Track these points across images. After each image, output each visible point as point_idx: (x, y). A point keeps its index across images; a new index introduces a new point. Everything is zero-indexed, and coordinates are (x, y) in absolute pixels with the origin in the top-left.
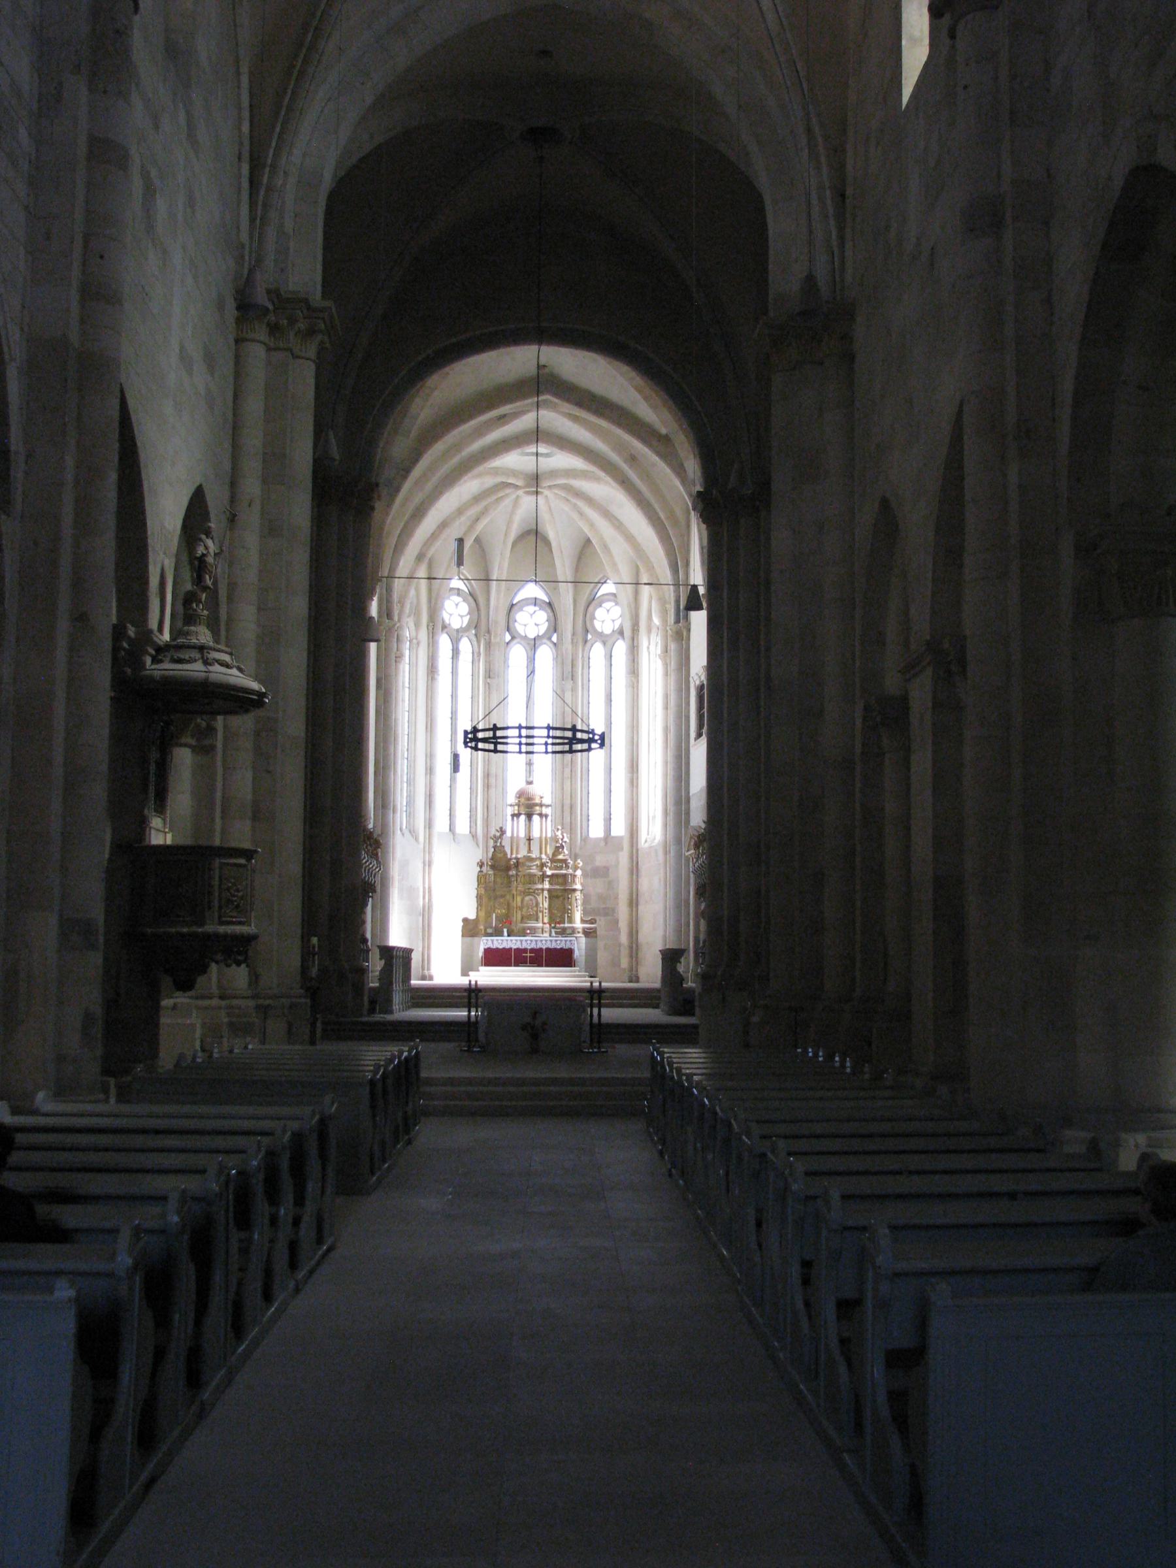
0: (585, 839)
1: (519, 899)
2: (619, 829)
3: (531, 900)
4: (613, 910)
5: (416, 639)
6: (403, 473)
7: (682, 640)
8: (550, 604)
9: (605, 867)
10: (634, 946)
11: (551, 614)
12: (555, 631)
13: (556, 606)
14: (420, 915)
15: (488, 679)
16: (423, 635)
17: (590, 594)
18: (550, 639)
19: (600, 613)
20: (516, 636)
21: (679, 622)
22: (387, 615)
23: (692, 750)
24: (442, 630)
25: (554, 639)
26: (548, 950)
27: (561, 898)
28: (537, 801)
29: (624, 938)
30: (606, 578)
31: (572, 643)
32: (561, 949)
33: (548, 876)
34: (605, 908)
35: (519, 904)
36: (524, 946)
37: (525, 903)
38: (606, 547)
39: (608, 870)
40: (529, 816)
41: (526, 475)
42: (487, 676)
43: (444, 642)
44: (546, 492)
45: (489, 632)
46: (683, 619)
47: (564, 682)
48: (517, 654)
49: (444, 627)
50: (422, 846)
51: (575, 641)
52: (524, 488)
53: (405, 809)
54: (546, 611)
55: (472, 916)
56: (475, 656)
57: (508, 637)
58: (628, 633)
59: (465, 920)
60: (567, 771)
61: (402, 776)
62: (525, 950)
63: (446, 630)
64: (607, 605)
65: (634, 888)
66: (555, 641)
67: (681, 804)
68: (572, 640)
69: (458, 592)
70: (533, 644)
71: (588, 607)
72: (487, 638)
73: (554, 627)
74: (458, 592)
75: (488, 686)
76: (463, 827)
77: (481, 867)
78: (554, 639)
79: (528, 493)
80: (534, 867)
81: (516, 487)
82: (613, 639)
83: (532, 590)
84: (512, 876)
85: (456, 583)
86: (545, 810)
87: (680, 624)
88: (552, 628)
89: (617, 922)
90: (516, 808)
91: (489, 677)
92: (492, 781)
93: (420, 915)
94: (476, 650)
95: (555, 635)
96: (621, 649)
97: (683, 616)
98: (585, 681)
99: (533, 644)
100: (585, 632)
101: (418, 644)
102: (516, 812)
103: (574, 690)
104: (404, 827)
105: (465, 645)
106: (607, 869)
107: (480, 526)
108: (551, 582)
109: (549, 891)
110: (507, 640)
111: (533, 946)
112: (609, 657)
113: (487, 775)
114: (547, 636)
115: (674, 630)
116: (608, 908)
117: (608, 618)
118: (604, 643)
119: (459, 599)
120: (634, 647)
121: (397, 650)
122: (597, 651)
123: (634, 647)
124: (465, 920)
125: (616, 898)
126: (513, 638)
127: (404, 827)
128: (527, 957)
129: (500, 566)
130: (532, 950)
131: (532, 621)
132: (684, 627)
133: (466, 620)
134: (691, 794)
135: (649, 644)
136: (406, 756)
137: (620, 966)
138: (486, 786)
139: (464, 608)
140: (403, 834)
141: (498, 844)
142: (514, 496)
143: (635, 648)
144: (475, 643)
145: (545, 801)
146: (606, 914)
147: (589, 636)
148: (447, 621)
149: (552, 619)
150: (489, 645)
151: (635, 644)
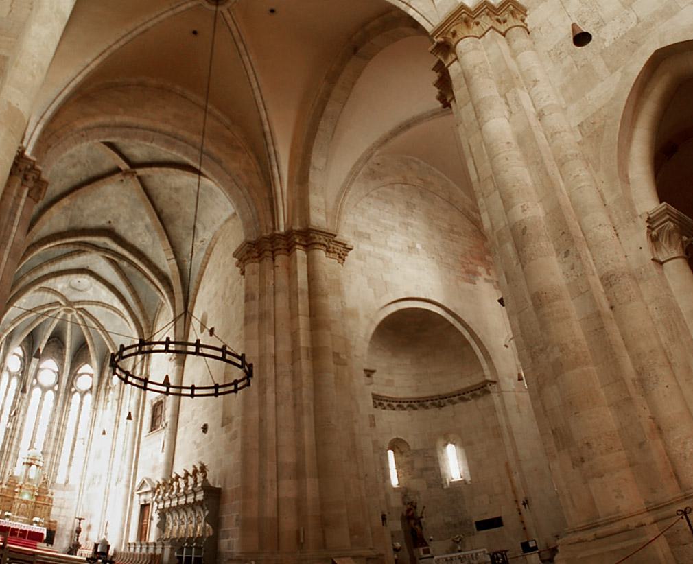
1: (18, 504)
25: (56, 388)
26: (30, 532)
32: (38, 533)
35: (17, 507)
36: (17, 527)
48: (37, 392)
49: (8, 370)
57: (35, 382)
58: (94, 389)
62: (17, 530)
70: (44, 390)
84: (17, 492)
95: (57, 386)
109: (35, 503)
111: (22, 528)
117: (83, 382)
118: (80, 393)
130: (21, 530)
142: (58, 311)
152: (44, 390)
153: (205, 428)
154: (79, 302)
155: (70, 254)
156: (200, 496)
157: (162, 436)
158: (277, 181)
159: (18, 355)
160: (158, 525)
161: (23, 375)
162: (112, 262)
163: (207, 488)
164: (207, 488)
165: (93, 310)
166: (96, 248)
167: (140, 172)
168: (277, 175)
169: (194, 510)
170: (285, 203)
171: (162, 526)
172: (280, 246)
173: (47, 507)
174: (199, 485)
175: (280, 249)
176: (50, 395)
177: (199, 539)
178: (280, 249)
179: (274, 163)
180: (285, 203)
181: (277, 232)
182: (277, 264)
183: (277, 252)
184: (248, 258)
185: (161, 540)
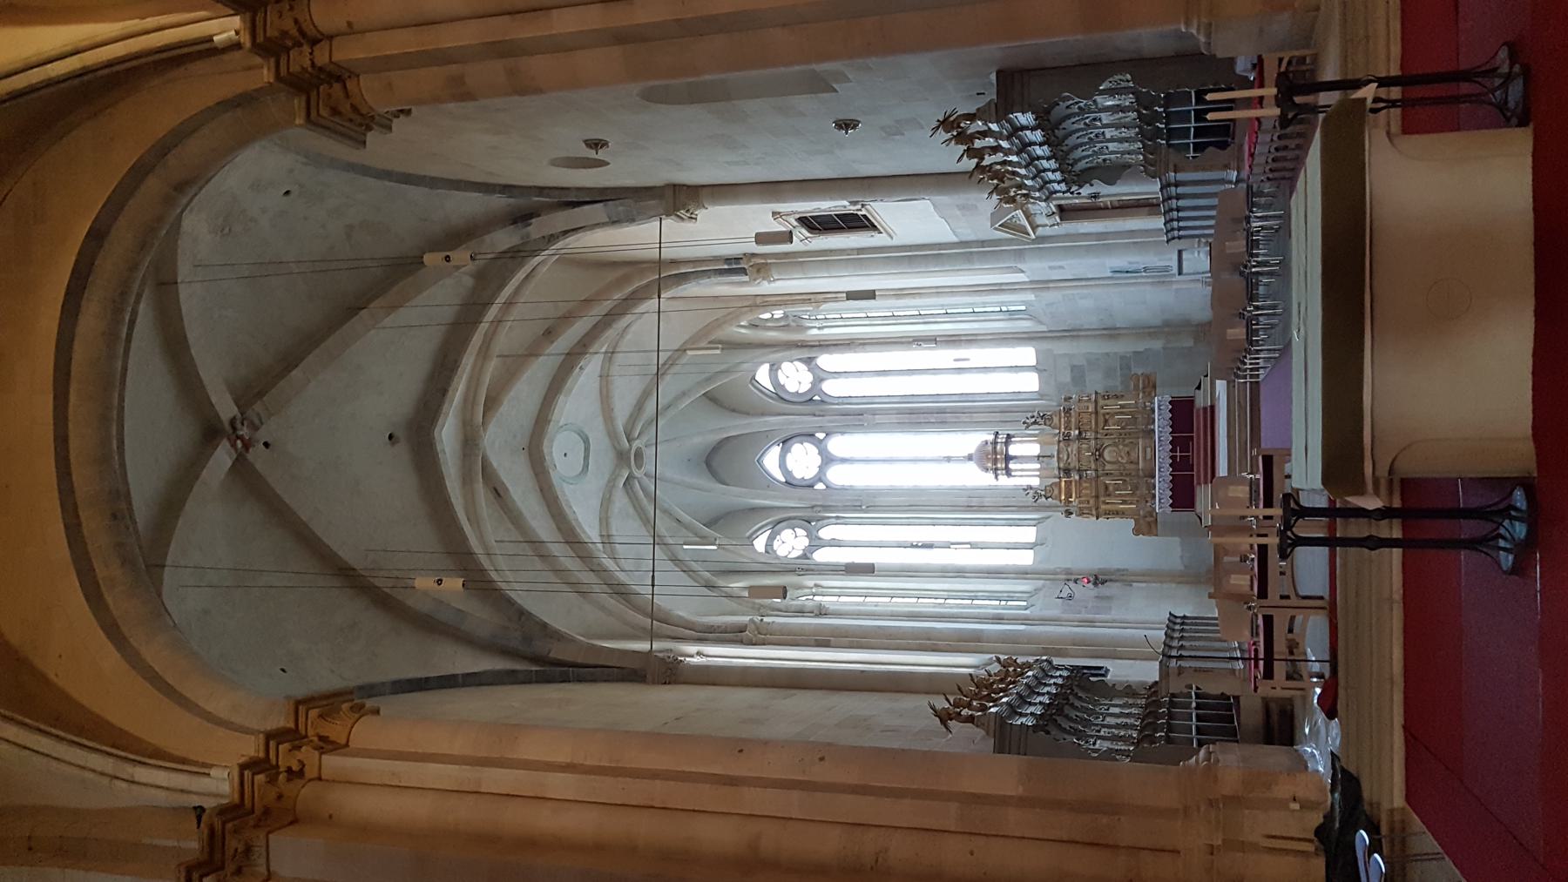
0: (1041, 395)
1: (1108, 467)
2: (1027, 355)
3: (1110, 452)
4: (1122, 358)
5: (812, 588)
6: (523, 618)
7: (767, 264)
8: (783, 442)
9: (1072, 371)
10: (1166, 329)
11: (794, 440)
12: (813, 435)
13: (784, 436)
14: (1131, 585)
15: (864, 507)
16: (809, 581)
17: (771, 398)
18: (821, 441)
19: (792, 387)
20: (817, 477)
21: (744, 268)
22: (741, 632)
23: (896, 242)
24: (808, 559)
25: (821, 436)
27: (1107, 417)
28: (990, 448)
29: (1157, 345)
30: (754, 381)
31: (823, 416)
33: (1080, 433)
34: (1121, 369)
35: (1115, 467)
37: (1114, 460)
38: (709, 380)
39: (1074, 366)
40: (1008, 458)
41: (617, 466)
42: (859, 508)
43: (822, 556)
44: (636, 444)
45: (813, 507)
46: (739, 264)
47: (866, 424)
48: (838, 476)
49: (805, 556)
50: (1048, 582)
51: (822, 413)
52: (630, 467)
53: (1003, 603)
54: (792, 445)
55: (1132, 523)
56: (839, 521)
57: (820, 486)
58: (806, 354)
59: (1137, 531)
60: (964, 418)
61: (964, 606)
63: (809, 555)
64: (782, 379)
65: (1094, 333)
66: (824, 435)
67: (971, 253)
68: (819, 416)
69: (771, 539)
71: (782, 398)
72: (819, 509)
73: (810, 436)
74: (769, 545)
75: (870, 509)
76: (1029, 534)
77: (1072, 513)
78: (821, 436)
79: (639, 466)
80: (1069, 450)
81: (630, 478)
82: (817, 371)
83: (771, 460)
85: (760, 544)
86: (1002, 439)
87: (746, 267)
88: (809, 438)
89: (1136, 353)
90: (999, 472)
91: (861, 506)
92: (975, 502)
93: (1131, 585)
94: (834, 521)
95: (818, 435)
96: (826, 361)
97: (735, 264)
98: (864, 400)
99: (828, 460)
100: (813, 402)
101: (816, 586)
102: (1004, 472)
103: (874, 412)
104: (1025, 603)
105: (826, 533)
106: (1073, 368)
107: (686, 518)
108: (760, 441)
110: (824, 487)
112: (837, 374)
113: (969, 508)
114: (819, 444)
115: (755, 275)
116: (1121, 365)
117: (795, 377)
118: (822, 380)
119: (776, 544)
120: (820, 346)
121: (812, 612)
122: (832, 388)
123: (820, 346)
124: (1137, 531)
125: (1107, 354)
126: (820, 480)
127: (1025, 603)
128: (1180, 456)
129: (734, 496)
131: (803, 460)
132: (749, 260)
133: (801, 532)
134: (955, 239)
135: (815, 327)
136: (942, 601)
137: (1191, 347)
138: (982, 509)
139: (787, 534)
140: (1032, 606)
141: (1043, 493)
143: (822, 343)
144: (825, 522)
145: (991, 438)
146: (1130, 369)
147: (817, 398)
148: (801, 553)
149: (798, 439)
150: (827, 508)
151: (817, 343)
152: (828, 460)
153: (846, 125)
154: (612, 434)
155: (498, 493)
156: (1025, 119)
157: (882, 210)
158: (90, 58)
159: (771, 539)
160: (1110, 182)
161: (810, 519)
162: (492, 403)
163: (1001, 108)
164: (1001, 108)
165: (622, 409)
166: (469, 442)
167: (226, 409)
168: (73, 64)
169: (1068, 153)
170: (151, 22)
171: (1112, 172)
172: (288, 24)
173: (1101, 402)
174: (994, 127)
175: (296, 21)
176: (837, 445)
177: (1142, 102)
178: (296, 21)
179: (36, 76)
180: (151, 22)
181: (246, 40)
182: (343, 26)
183: (310, 31)
184: (355, 108)
185: (1152, 168)
